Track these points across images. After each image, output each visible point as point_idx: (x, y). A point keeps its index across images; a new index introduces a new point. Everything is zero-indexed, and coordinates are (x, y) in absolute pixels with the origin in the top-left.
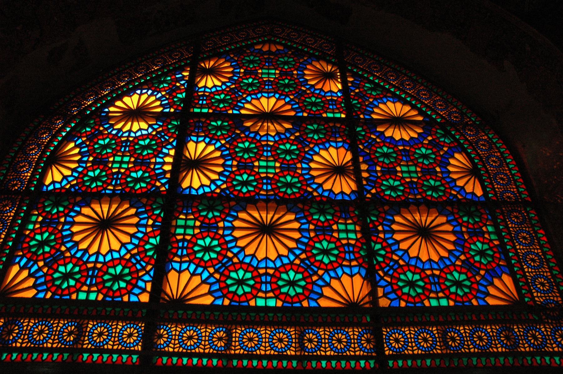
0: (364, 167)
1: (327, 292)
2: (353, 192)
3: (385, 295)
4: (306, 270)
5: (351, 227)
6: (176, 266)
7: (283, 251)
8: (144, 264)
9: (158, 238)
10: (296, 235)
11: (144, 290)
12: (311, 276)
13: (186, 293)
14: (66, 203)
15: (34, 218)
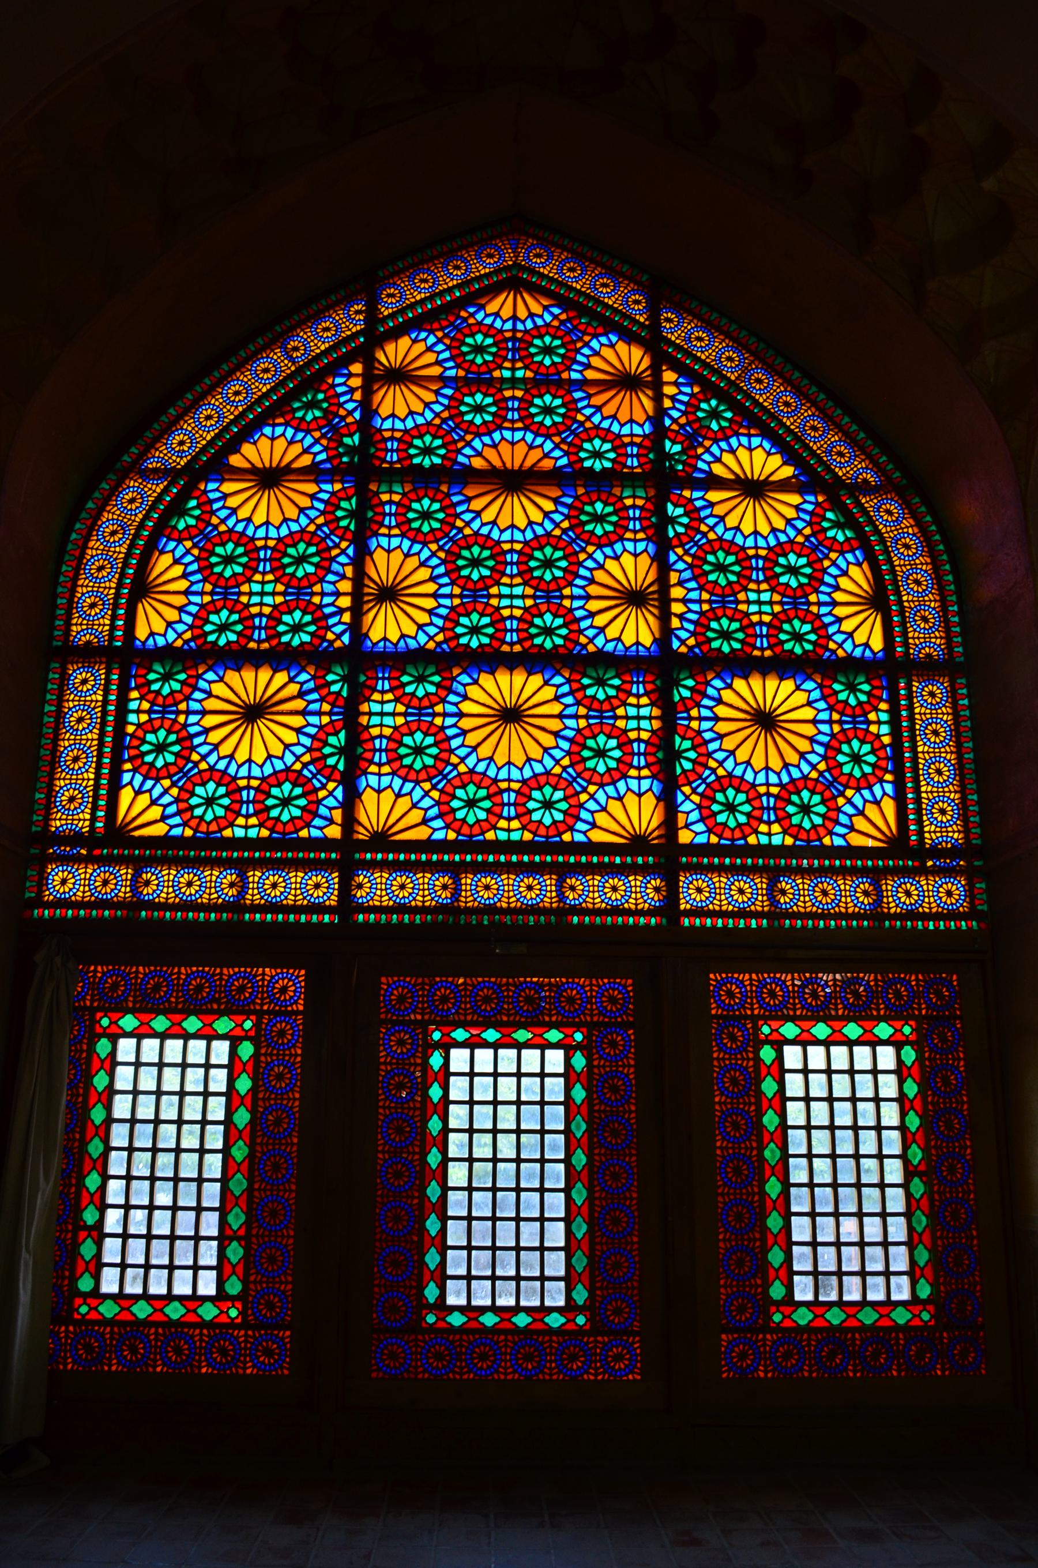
0: (677, 592)
1: (602, 819)
2: (655, 640)
3: (687, 826)
4: (570, 784)
5: (645, 712)
6: (373, 780)
7: (535, 752)
8: (324, 781)
9: (342, 735)
10: (555, 725)
11: (331, 821)
12: (577, 794)
13: (390, 822)
14: (182, 676)
15: (133, 705)
